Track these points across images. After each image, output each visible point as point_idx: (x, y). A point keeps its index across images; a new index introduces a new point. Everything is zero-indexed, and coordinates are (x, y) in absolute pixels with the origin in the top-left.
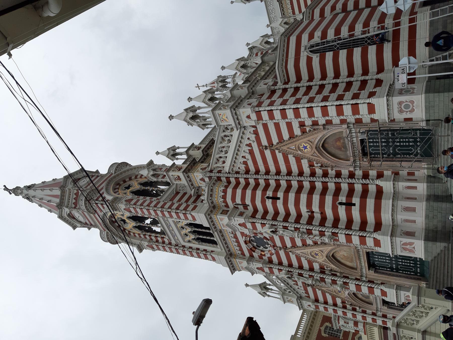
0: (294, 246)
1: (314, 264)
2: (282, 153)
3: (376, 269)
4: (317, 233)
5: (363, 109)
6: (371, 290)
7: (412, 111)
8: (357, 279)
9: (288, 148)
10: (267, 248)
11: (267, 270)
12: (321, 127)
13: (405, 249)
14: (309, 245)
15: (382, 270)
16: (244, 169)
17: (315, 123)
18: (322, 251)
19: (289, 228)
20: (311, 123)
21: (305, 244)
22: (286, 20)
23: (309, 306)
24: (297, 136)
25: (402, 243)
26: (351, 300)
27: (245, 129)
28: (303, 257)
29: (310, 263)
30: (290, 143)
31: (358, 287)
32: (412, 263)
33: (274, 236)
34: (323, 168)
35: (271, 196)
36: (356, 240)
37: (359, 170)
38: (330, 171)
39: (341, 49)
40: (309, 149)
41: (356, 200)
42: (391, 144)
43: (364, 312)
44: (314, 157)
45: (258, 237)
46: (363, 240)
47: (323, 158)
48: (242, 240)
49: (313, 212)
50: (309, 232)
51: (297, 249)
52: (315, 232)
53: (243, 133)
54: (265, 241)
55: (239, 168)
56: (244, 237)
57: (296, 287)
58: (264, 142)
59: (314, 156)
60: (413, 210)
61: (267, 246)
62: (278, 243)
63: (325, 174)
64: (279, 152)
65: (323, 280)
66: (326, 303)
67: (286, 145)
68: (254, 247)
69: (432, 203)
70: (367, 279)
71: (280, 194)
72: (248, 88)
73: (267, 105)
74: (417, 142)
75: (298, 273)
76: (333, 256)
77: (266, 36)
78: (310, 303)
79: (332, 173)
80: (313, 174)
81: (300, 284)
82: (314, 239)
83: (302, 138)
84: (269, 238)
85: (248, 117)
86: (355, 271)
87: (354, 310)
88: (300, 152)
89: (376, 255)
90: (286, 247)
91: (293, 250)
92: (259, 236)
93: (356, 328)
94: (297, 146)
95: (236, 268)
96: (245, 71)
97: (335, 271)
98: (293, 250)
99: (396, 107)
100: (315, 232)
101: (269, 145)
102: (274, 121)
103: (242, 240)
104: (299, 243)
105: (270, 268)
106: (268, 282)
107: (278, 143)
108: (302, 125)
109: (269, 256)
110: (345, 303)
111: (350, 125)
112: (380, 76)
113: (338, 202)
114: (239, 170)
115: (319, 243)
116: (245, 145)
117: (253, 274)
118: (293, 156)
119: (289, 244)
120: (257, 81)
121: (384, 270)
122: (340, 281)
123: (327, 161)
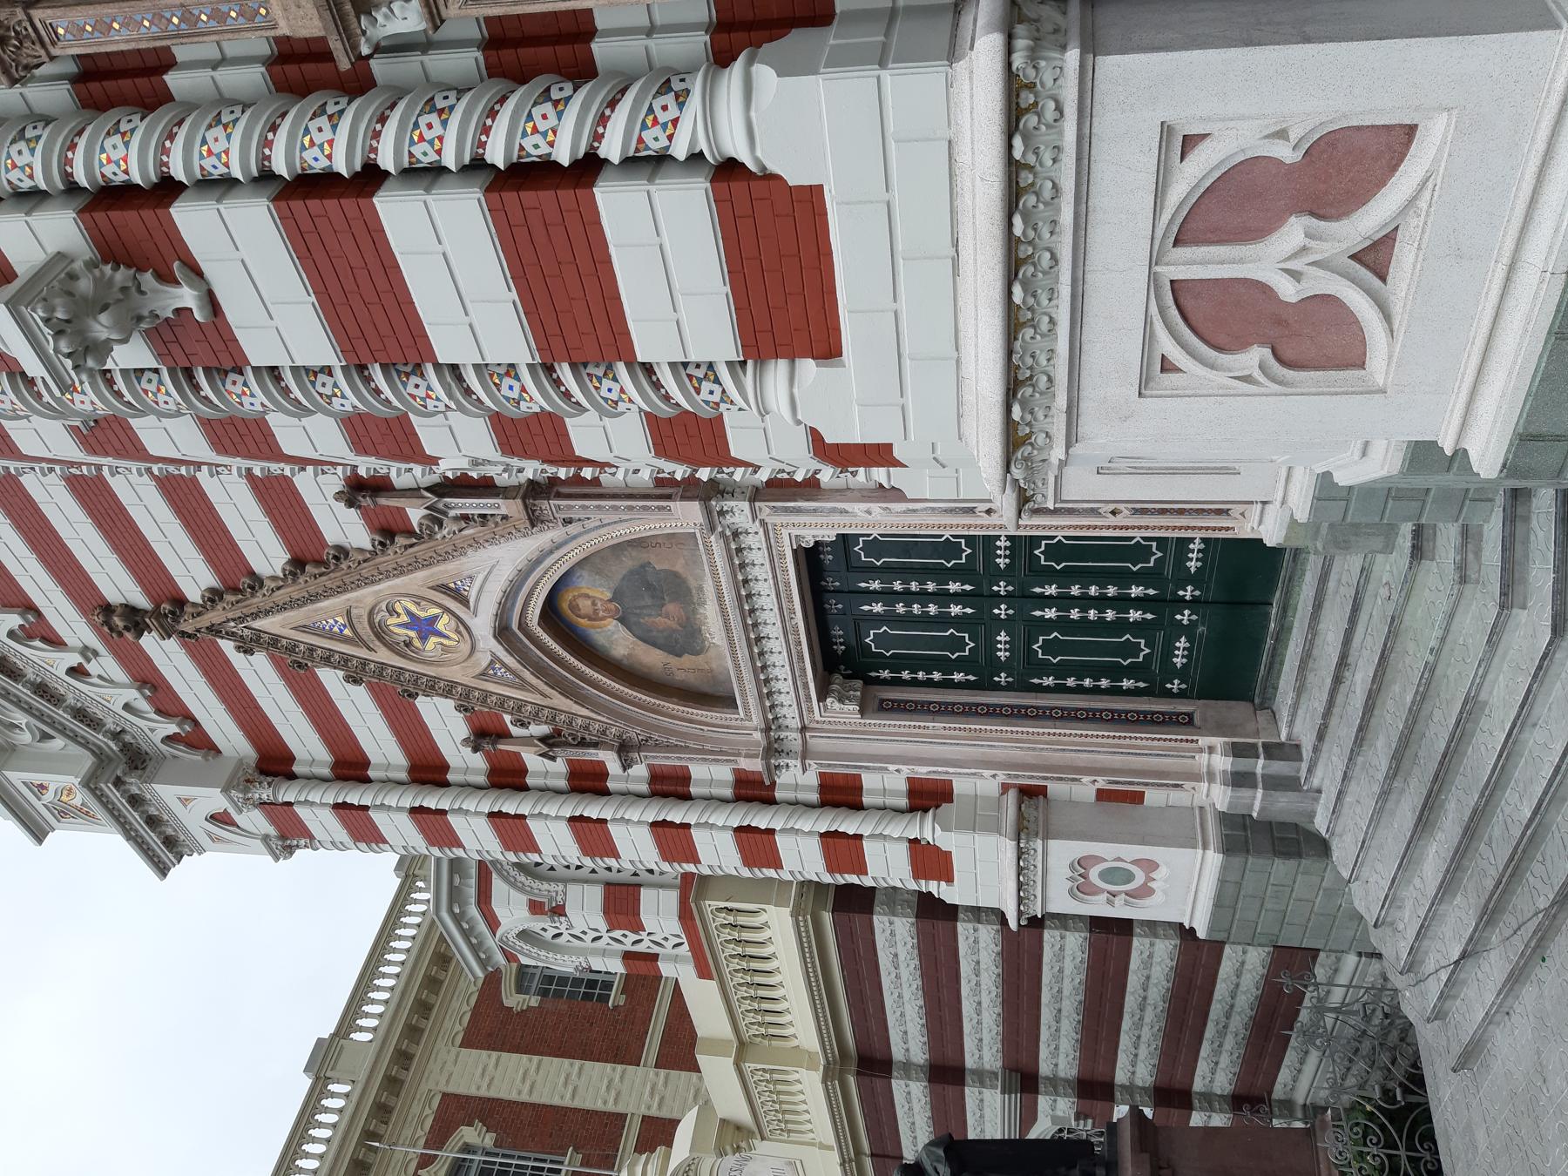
24: (342, 552)
42: (1002, 611)
107: (214, 596)
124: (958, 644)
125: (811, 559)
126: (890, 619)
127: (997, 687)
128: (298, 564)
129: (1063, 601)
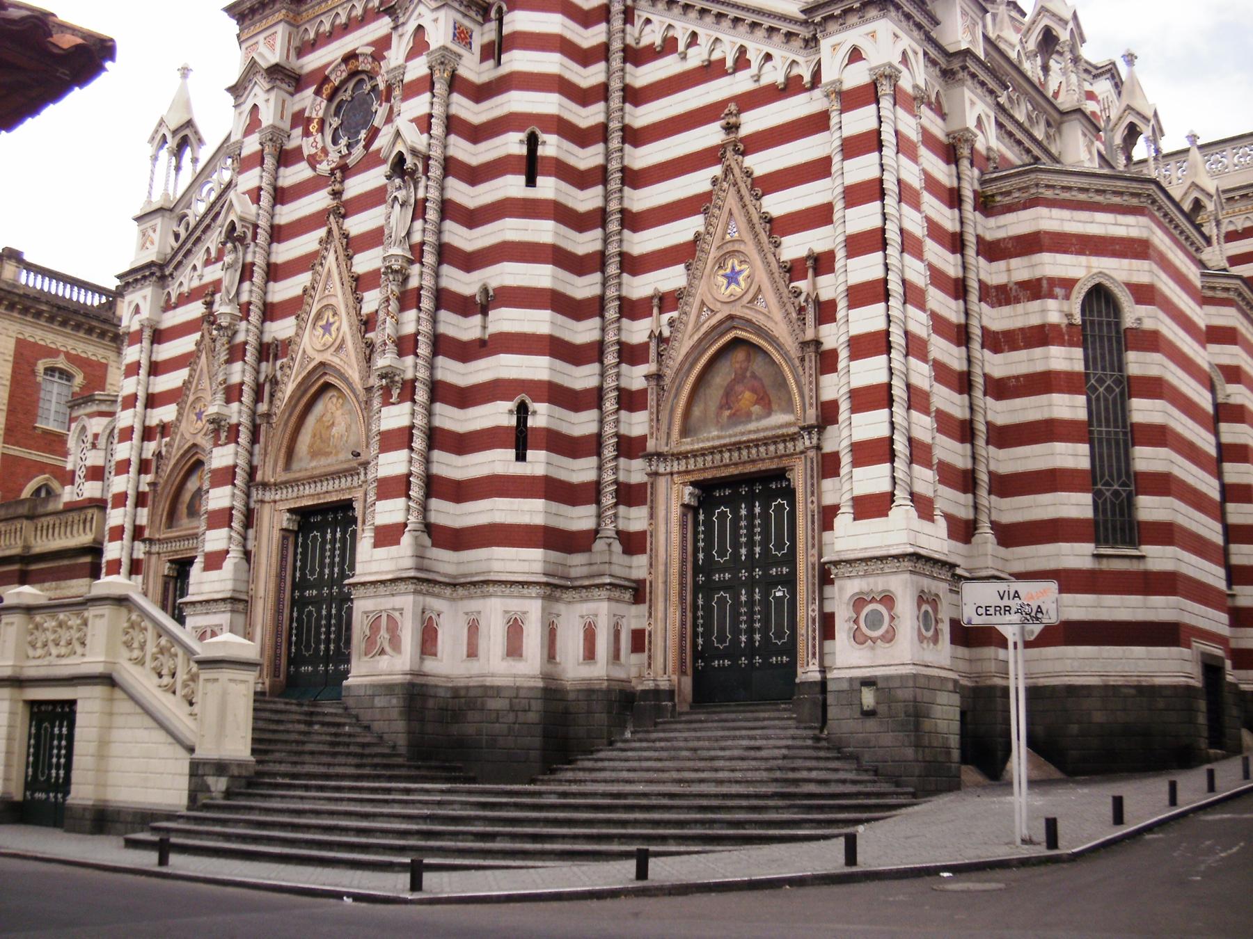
0: (353, 245)
1: (291, 321)
2: (710, 193)
3: (296, 533)
4: (409, 329)
5: (873, 479)
6: (222, 518)
7: (858, 638)
8: (252, 472)
9: (731, 214)
10: (335, 142)
11: (251, 145)
12: (810, 334)
13: (374, 626)
14: (359, 300)
15: (295, 554)
16: (645, 42)
17: (826, 312)
18: (340, 347)
19: (418, 224)
20: (825, 296)
21: (360, 284)
22: (1210, 206)
23: (137, 310)
24: (777, 245)
25: (396, 615)
26: (176, 454)
27: (807, 42)
28: (314, 280)
29: (293, 307)
30: (750, 221)
31: (226, 476)
32: (327, 649)
33: (385, 169)
34: (653, 346)
35: (541, 151)
36: (393, 463)
37: (648, 470)
38: (643, 369)
39: (1089, 401)
40: (724, 290)
41: (538, 463)
42: (744, 574)
43: (141, 500)
44: (694, 312)
45: (375, 106)
46: (394, 487)
47: (691, 343)
48: (359, 40)
49: (484, 311)
50: (408, 299)
51: (341, 257)
52: (410, 322)
53: (789, 35)
54: (363, 134)
55: (648, 21)
56: (370, 50)
57: (198, 258)
58: (754, 121)
59: (700, 310)
60: (514, 649)
61: (343, 141)
62: (356, 186)
63: (632, 355)
64: (715, 181)
65: (236, 353)
66: (156, 369)
67: (744, 206)
68: (336, 91)
69: (537, 705)
70: (257, 506)
71: (547, 187)
72: (967, 52)
73: (902, 128)
74: (751, 658)
75: (253, 264)
76: (327, 386)
77: (1158, 132)
78: (145, 313)
79: (636, 377)
80: (632, 309)
81: (213, 273)
82: (382, 315)
83: (768, 264)
84: (374, 147)
85: (855, 55)
86: (281, 463)
87: (144, 467)
88: (713, 254)
89: (344, 533)
90: (344, 216)
91: (337, 242)
92: (381, 111)
93: (81, 473)
94: (737, 247)
95: (247, 22)
96: (1032, 45)
97: (272, 395)
98: (337, 242)
99: (877, 584)
100: (410, 322)
101: (741, 140)
102: (837, 159)
103: (359, 40)
104: (366, 262)
105: (258, 159)
106: (205, 154)
107: (748, 174)
108: (821, 263)
109: (307, 151)
110: (163, 436)
111: (815, 437)
112: (986, 534)
113: (528, 401)
114: (638, 23)
115: (370, 335)
116: (740, 42)
117: (230, 90)
118: (698, 236)
119: (357, 224)
120: (991, 92)
121: (295, 561)
122: (236, 413)
123: (680, 358)
124: (722, 553)
125: (781, 474)
126: (736, 518)
127: (695, 575)
128: (770, 220)
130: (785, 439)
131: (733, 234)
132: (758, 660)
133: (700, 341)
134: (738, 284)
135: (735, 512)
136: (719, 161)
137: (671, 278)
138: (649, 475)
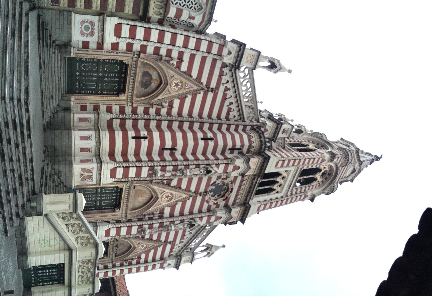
9: (192, 87)
24: (179, 99)
42: (101, 75)
58: (210, 95)
64: (202, 84)
107: (199, 93)
118: (191, 76)
129: (93, 76)
130: (132, 96)
131: (187, 86)
132: (78, 78)
133: (165, 74)
134: (175, 83)
135: (117, 73)
136: (206, 86)
137: (184, 67)
138: (134, 52)
